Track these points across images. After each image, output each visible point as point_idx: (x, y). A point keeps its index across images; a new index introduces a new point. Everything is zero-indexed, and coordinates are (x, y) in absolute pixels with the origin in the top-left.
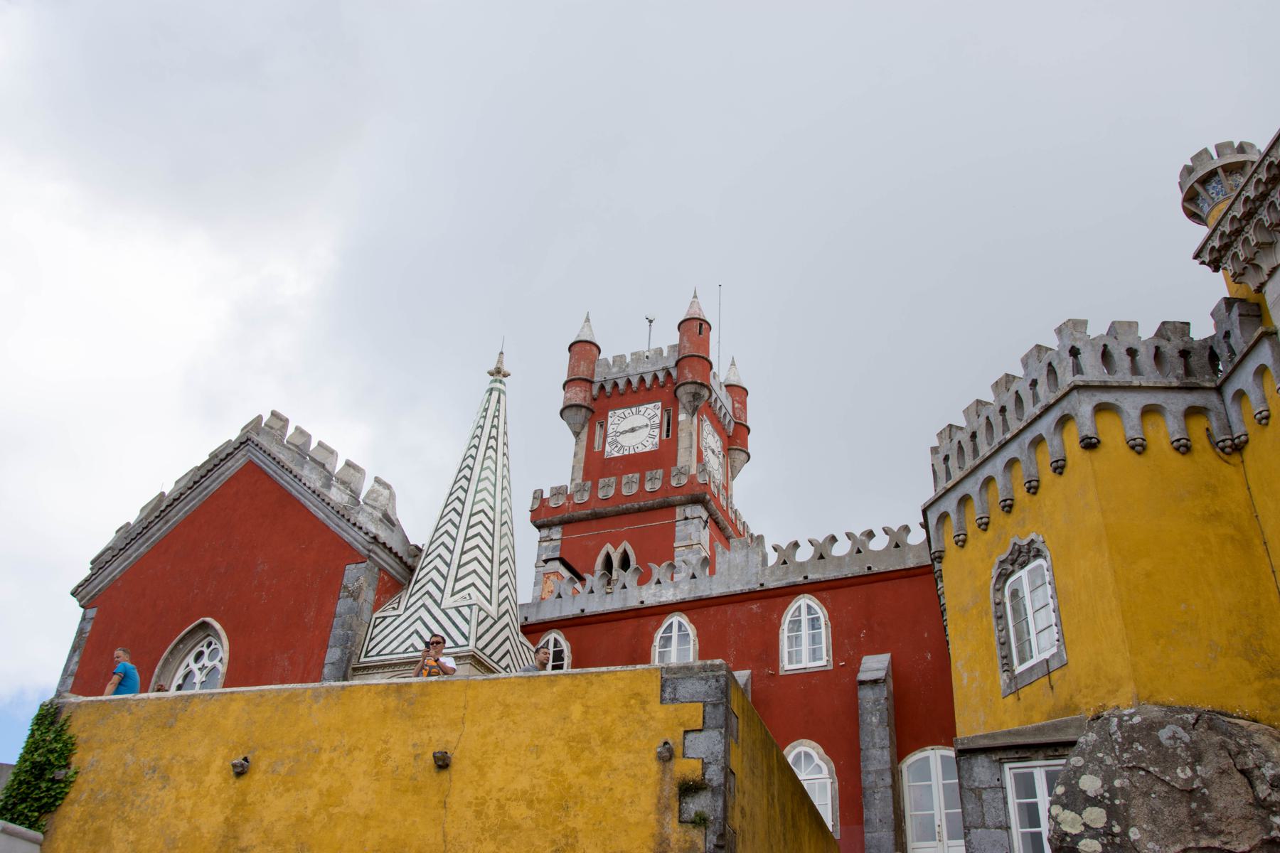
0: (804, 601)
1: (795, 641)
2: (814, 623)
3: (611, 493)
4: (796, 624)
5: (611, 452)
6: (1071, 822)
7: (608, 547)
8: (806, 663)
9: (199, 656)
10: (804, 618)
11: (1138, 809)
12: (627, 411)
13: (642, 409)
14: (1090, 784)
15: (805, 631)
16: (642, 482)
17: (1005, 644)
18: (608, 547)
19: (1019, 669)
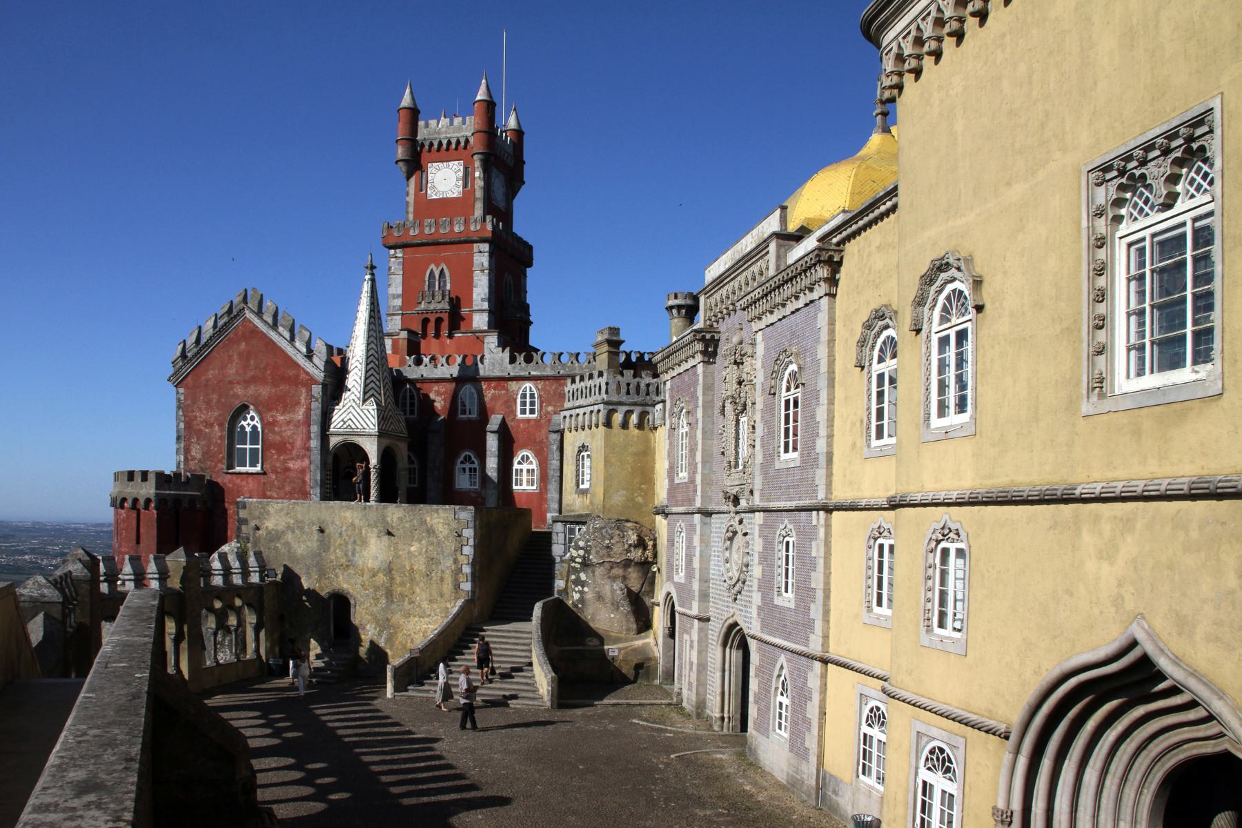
0: (528, 385)
1: (524, 404)
2: (532, 396)
3: (433, 230)
4: (524, 396)
5: (432, 195)
6: (574, 553)
7: (432, 266)
8: (528, 415)
9: (245, 419)
10: (528, 393)
11: (593, 551)
12: (440, 164)
13: (451, 164)
14: (581, 544)
15: (528, 400)
16: (451, 223)
17: (578, 475)
18: (432, 266)
19: (581, 487)
